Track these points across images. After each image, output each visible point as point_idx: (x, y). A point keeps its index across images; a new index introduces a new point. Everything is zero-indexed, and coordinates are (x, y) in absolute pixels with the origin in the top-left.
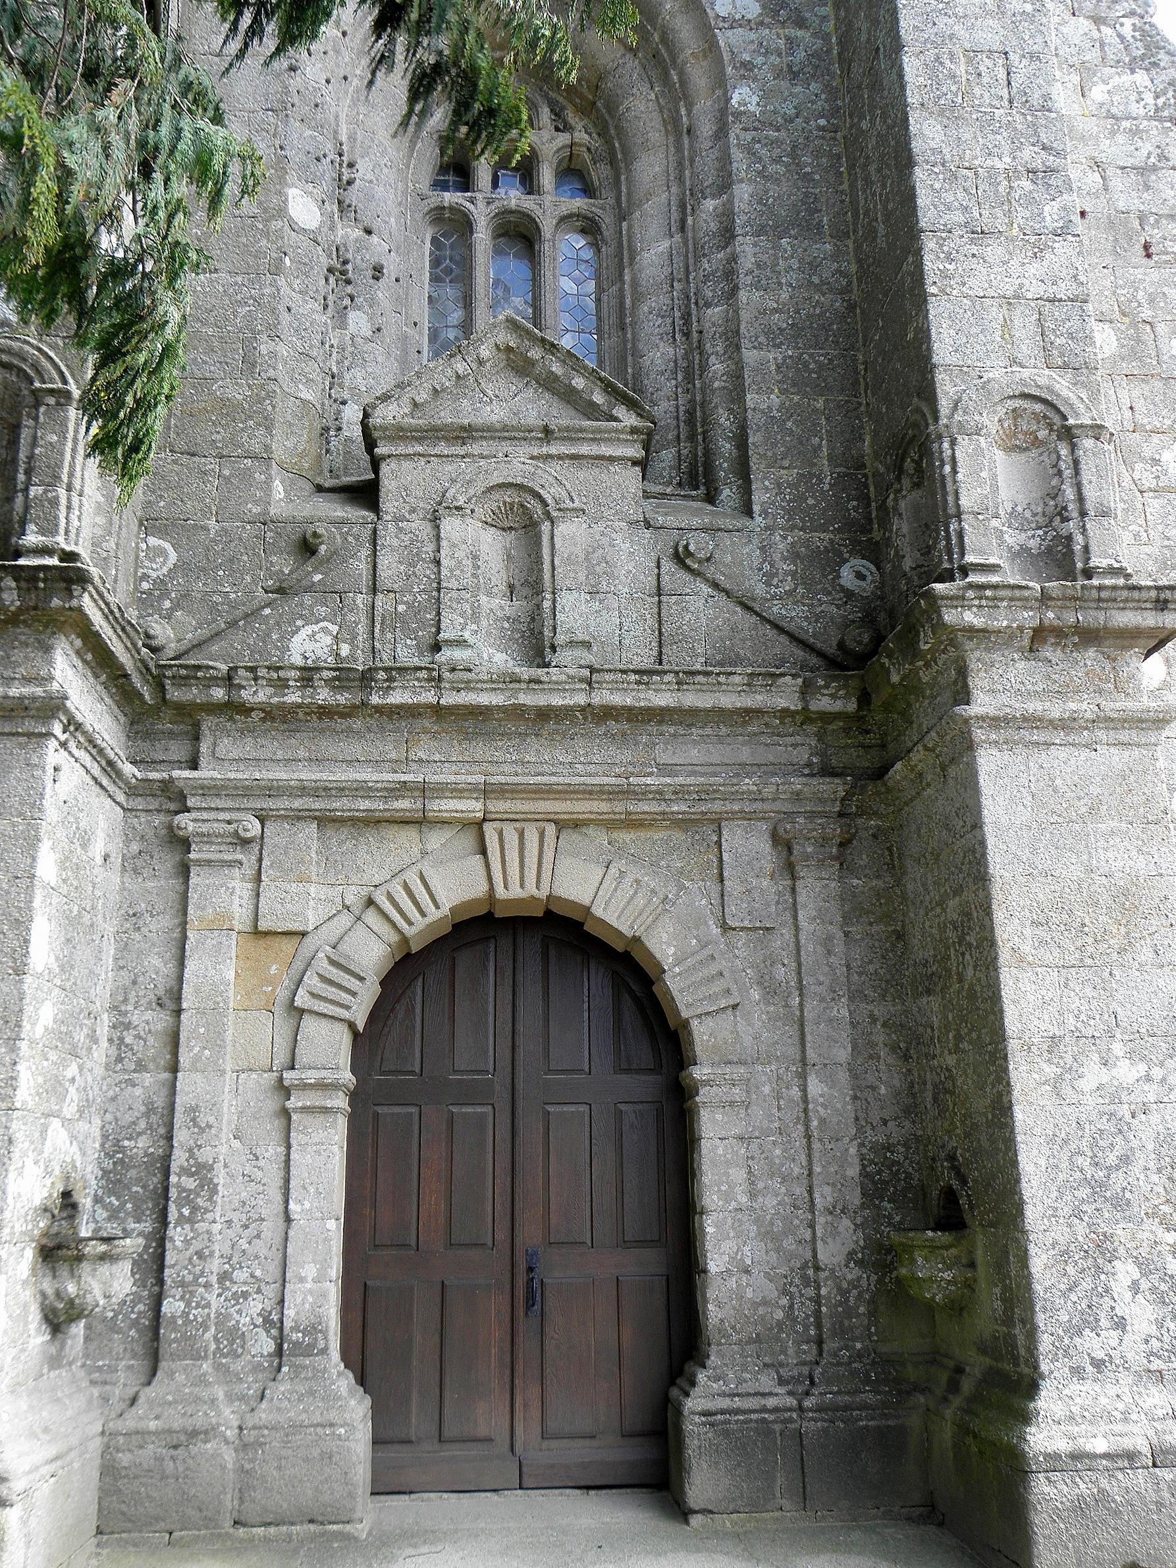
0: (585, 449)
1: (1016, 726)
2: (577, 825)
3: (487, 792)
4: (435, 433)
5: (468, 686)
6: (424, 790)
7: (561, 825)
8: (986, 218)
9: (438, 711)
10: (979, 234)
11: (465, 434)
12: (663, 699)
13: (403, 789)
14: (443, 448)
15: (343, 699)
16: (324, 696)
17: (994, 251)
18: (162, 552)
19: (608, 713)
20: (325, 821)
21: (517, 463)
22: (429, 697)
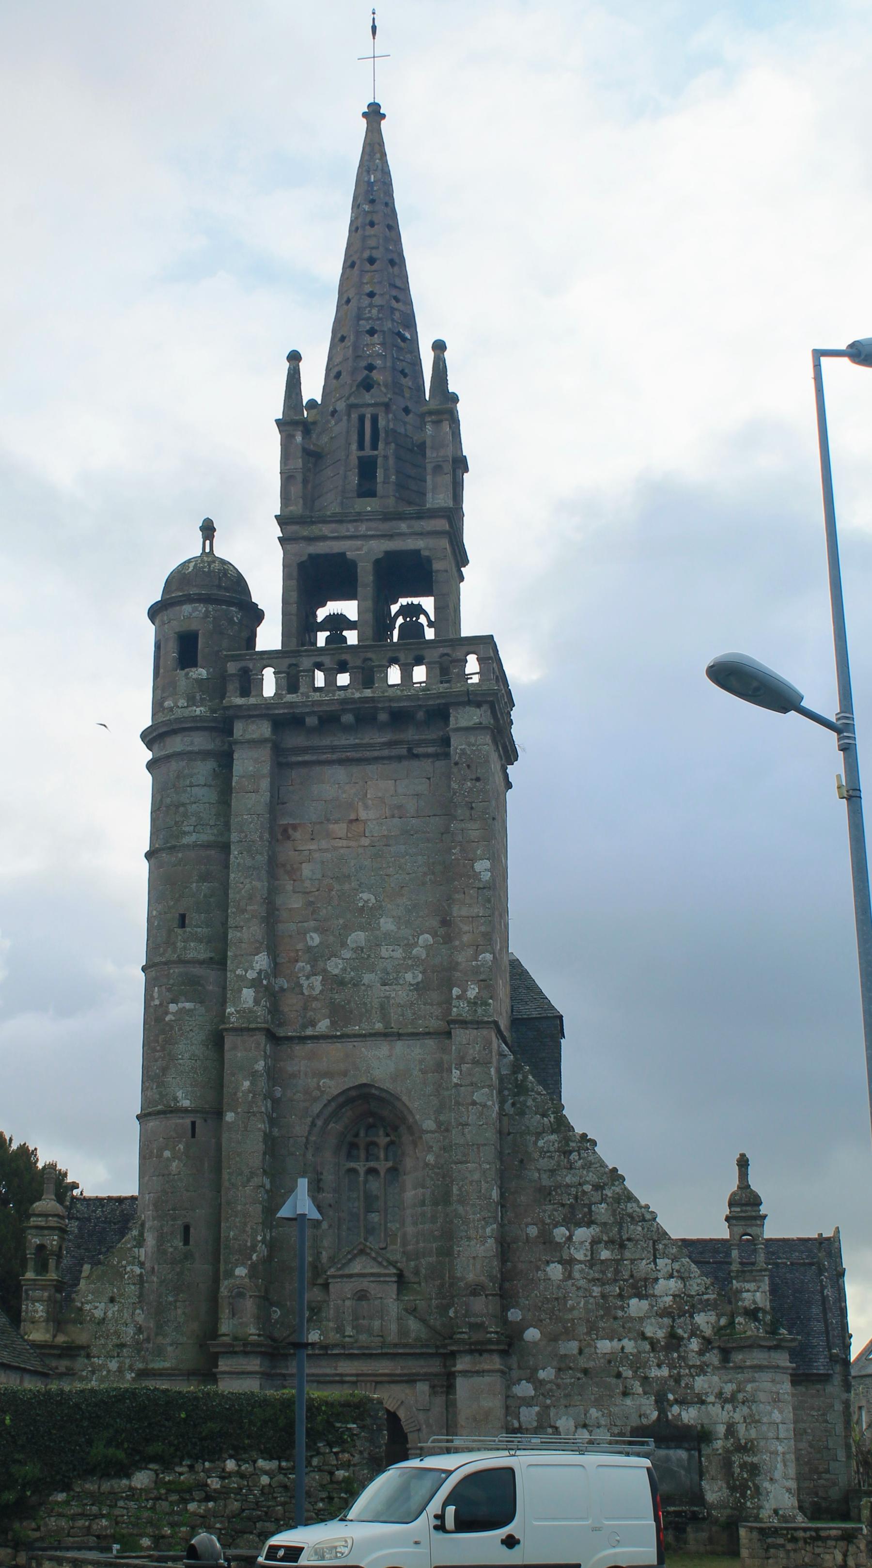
0: (382, 1279)
1: (465, 1373)
2: (381, 1382)
3: (357, 1375)
4: (342, 1276)
5: (352, 1348)
6: (341, 1375)
7: (377, 1383)
8: (472, 1233)
9: (344, 1354)
10: (469, 1239)
11: (351, 1276)
12: (400, 1351)
13: (337, 1375)
14: (345, 1280)
15: (321, 1352)
16: (317, 1352)
17: (473, 1243)
18: (276, 1312)
19: (386, 1354)
20: (319, 1382)
21: (364, 1284)
22: (342, 1352)
